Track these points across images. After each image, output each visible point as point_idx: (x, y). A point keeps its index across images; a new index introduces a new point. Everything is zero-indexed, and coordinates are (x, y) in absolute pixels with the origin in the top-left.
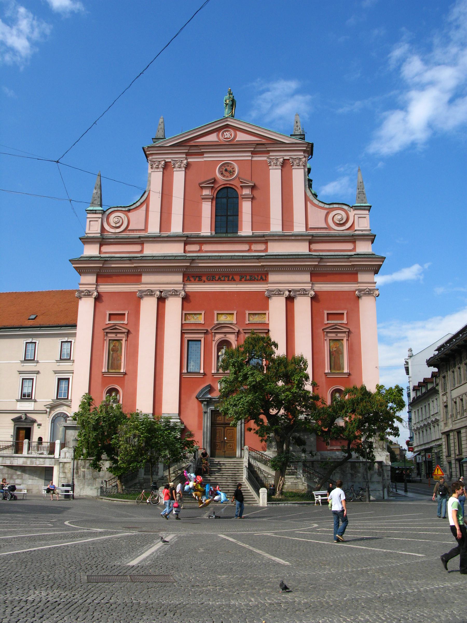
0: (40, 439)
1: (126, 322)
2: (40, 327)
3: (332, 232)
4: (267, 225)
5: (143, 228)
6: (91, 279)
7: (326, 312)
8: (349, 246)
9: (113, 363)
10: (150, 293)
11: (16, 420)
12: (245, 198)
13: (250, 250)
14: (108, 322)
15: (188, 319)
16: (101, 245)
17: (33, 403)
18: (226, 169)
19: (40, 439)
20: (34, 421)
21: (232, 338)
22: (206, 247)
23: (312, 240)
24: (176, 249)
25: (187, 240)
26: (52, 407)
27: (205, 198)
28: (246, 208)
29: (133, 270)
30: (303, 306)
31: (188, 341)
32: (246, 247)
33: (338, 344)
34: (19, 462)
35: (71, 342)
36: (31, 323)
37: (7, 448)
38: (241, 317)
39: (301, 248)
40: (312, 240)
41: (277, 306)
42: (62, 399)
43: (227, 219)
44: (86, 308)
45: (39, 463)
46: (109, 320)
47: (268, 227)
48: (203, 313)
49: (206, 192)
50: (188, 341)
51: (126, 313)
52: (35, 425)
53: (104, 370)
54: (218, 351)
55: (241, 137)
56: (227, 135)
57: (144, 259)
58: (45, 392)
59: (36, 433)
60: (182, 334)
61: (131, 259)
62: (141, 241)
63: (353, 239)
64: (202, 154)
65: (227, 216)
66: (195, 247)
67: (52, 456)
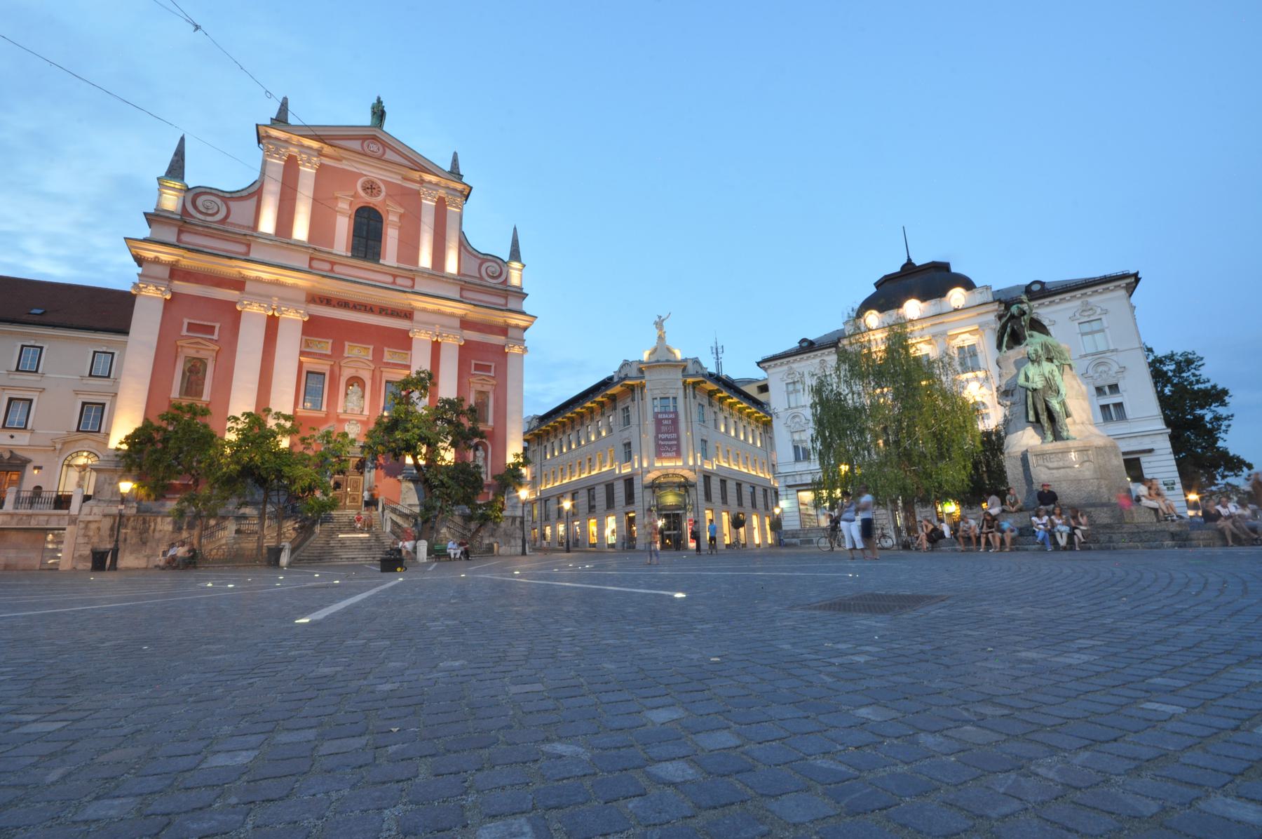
1: (215, 337)
5: (251, 224)
15: (308, 345)
16: (180, 232)
17: (28, 435)
18: (371, 188)
21: (366, 376)
22: (337, 268)
27: (343, 213)
28: (391, 237)
31: (308, 372)
32: (390, 279)
35: (113, 354)
38: (378, 355)
46: (188, 330)
48: (330, 341)
49: (343, 205)
50: (308, 372)
51: (217, 326)
52: (29, 467)
56: (374, 147)
65: (367, 239)
66: (327, 266)
67: (65, 512)
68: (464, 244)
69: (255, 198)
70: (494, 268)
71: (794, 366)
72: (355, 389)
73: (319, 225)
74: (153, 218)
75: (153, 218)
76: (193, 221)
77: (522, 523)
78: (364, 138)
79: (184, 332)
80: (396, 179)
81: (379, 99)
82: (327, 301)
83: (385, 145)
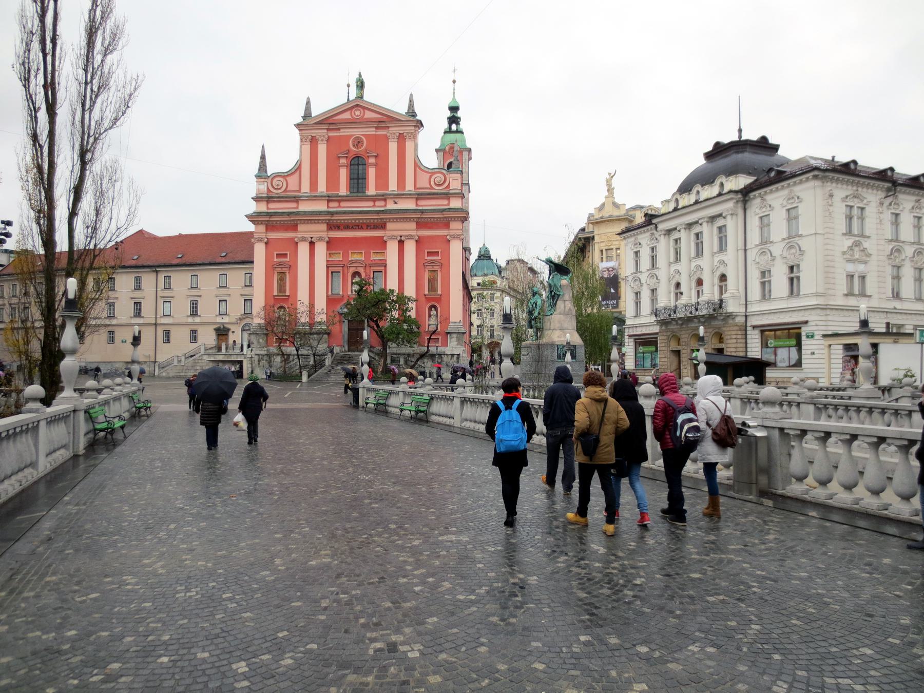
2: (229, 263)
3: (433, 191)
4: (386, 186)
6: (262, 228)
8: (445, 202)
9: (282, 289)
10: (304, 239)
11: (217, 330)
12: (372, 165)
13: (374, 206)
14: (275, 260)
18: (358, 142)
20: (229, 330)
21: (361, 270)
22: (342, 204)
23: (419, 197)
24: (322, 206)
25: (329, 199)
26: (241, 319)
28: (372, 172)
29: (291, 223)
30: (410, 248)
32: (371, 204)
33: (434, 274)
34: (220, 358)
36: (223, 260)
37: (211, 348)
38: (367, 255)
39: (410, 205)
40: (419, 197)
41: (392, 248)
42: (248, 315)
43: (357, 182)
44: (259, 252)
45: (233, 358)
47: (387, 189)
49: (343, 161)
53: (275, 293)
54: (353, 278)
55: (369, 115)
56: (358, 113)
57: (298, 213)
58: (235, 309)
60: (328, 267)
61: (289, 214)
62: (296, 200)
63: (447, 196)
64: (339, 129)
65: (358, 179)
66: (335, 204)
68: (417, 165)
69: (298, 173)
70: (439, 178)
71: (639, 237)
73: (332, 180)
74: (257, 199)
75: (257, 199)
76: (273, 195)
77: (458, 358)
78: (351, 109)
79: (275, 260)
80: (372, 131)
81: (360, 75)
82: (338, 227)
83: (364, 108)
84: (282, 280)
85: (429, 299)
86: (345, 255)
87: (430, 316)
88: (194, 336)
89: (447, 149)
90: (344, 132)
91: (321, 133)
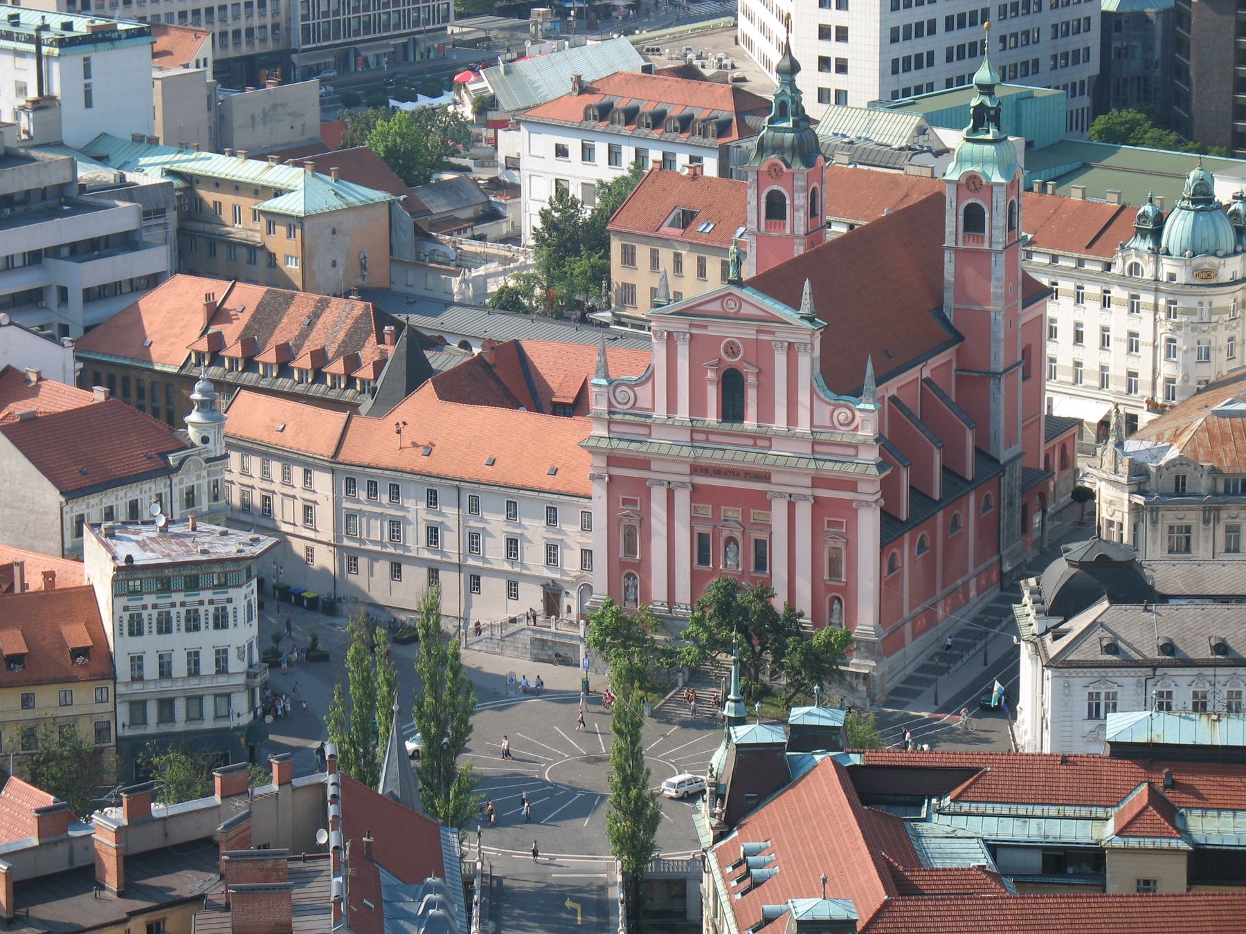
0: (569, 607)
7: (826, 519)
9: (630, 549)
18: (732, 349)
19: (569, 607)
21: (738, 535)
28: (751, 395)
30: (804, 513)
38: (746, 514)
41: (779, 511)
43: (732, 409)
49: (711, 375)
56: (731, 304)
58: (571, 562)
59: (565, 601)
60: (692, 528)
72: (732, 546)
80: (751, 334)
84: (630, 535)
85: (830, 589)
86: (716, 511)
87: (831, 611)
88: (513, 592)
89: (963, 181)
90: (715, 330)
91: (680, 325)
